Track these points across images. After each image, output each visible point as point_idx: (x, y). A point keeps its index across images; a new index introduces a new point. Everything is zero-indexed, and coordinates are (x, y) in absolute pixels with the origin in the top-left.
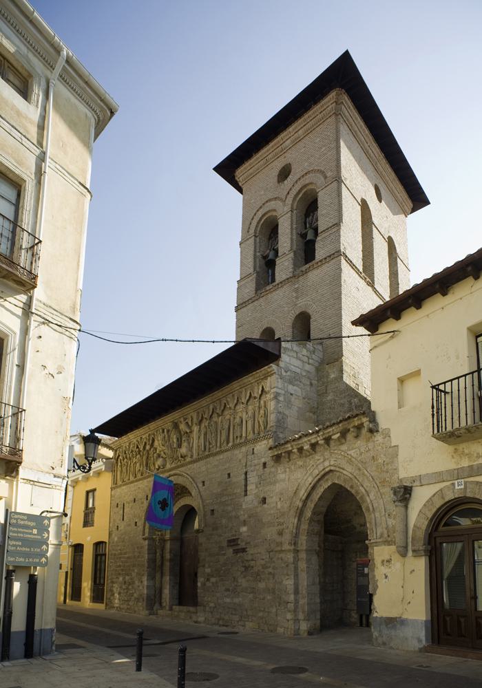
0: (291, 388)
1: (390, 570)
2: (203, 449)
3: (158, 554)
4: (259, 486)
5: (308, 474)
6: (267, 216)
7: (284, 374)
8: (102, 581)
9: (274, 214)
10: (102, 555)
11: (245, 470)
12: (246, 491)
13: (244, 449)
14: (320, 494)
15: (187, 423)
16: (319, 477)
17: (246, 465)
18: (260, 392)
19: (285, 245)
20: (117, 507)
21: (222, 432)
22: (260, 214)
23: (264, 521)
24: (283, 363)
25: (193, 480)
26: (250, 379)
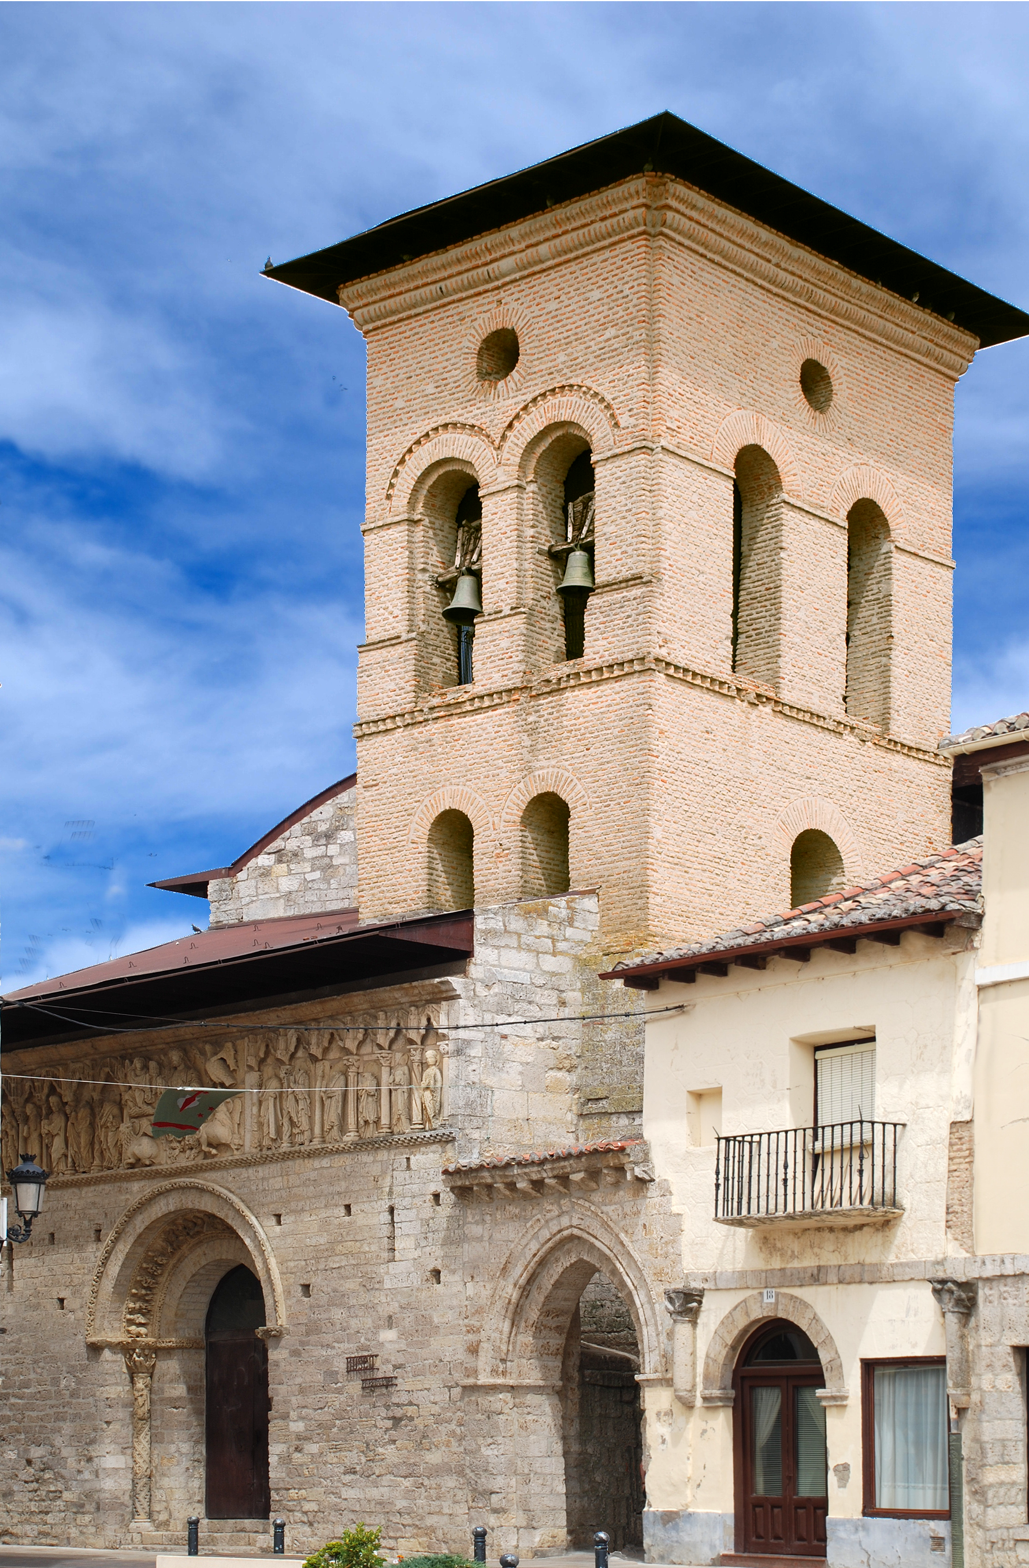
2: (273, 1135)
19: (501, 584)
24: (480, 969)
26: (397, 995)
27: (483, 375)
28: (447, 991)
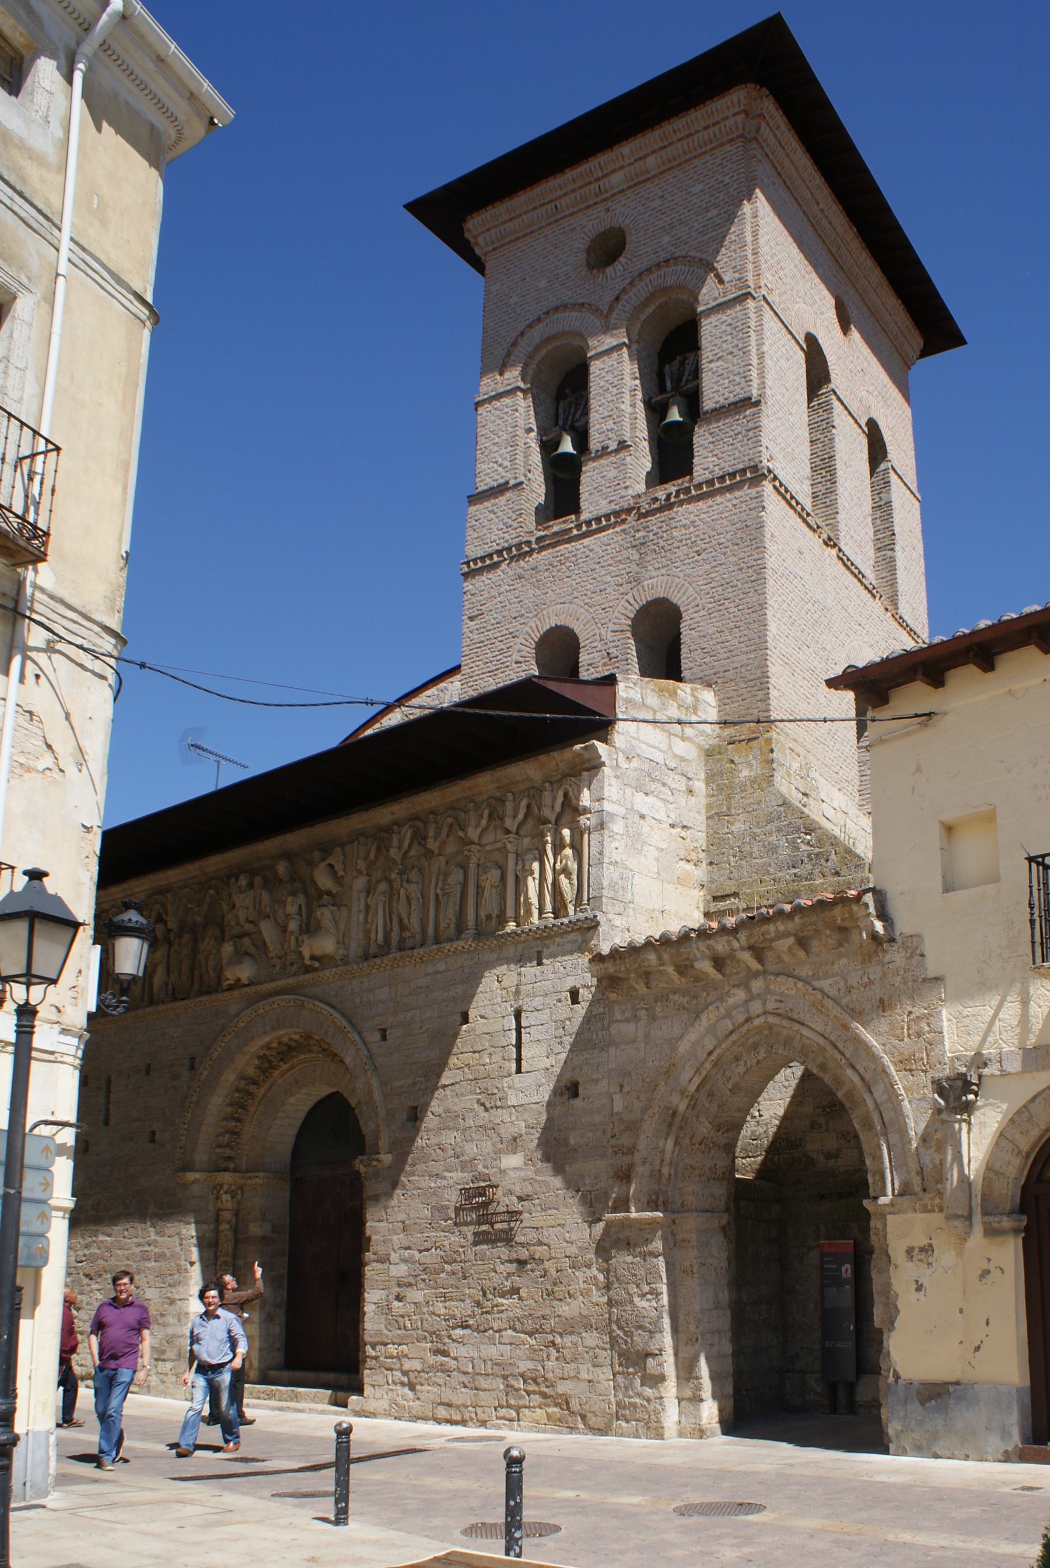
0: (642, 803)
1: (929, 1271)
6: (557, 343)
7: (624, 764)
9: (576, 342)
12: (519, 1060)
17: (517, 992)
18: (558, 808)
22: (536, 335)
23: (572, 1141)
25: (351, 1023)
27: (591, 267)
28: (589, 760)
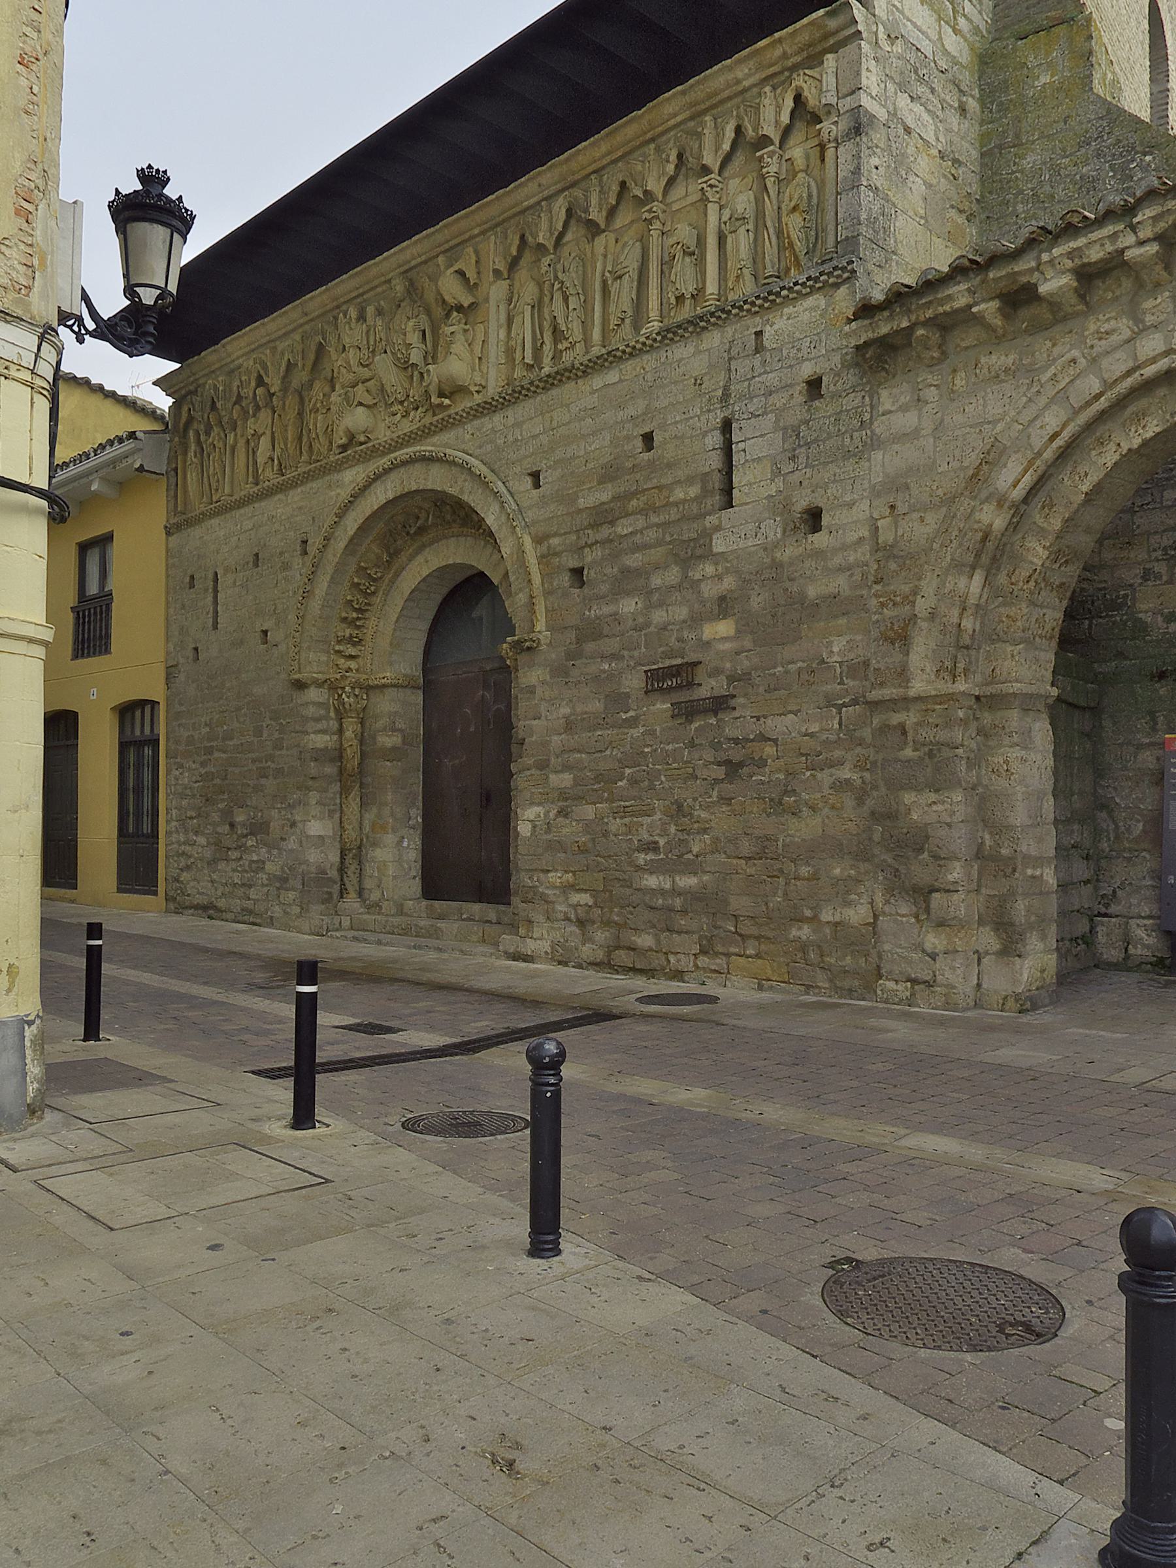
3: (349, 734)
4: (787, 468)
5: (1042, 401)
8: (146, 828)
10: (140, 744)
11: (720, 415)
13: (714, 340)
14: (1094, 477)
15: (461, 273)
16: (1103, 403)
17: (726, 396)
20: (192, 586)
21: (614, 288)
